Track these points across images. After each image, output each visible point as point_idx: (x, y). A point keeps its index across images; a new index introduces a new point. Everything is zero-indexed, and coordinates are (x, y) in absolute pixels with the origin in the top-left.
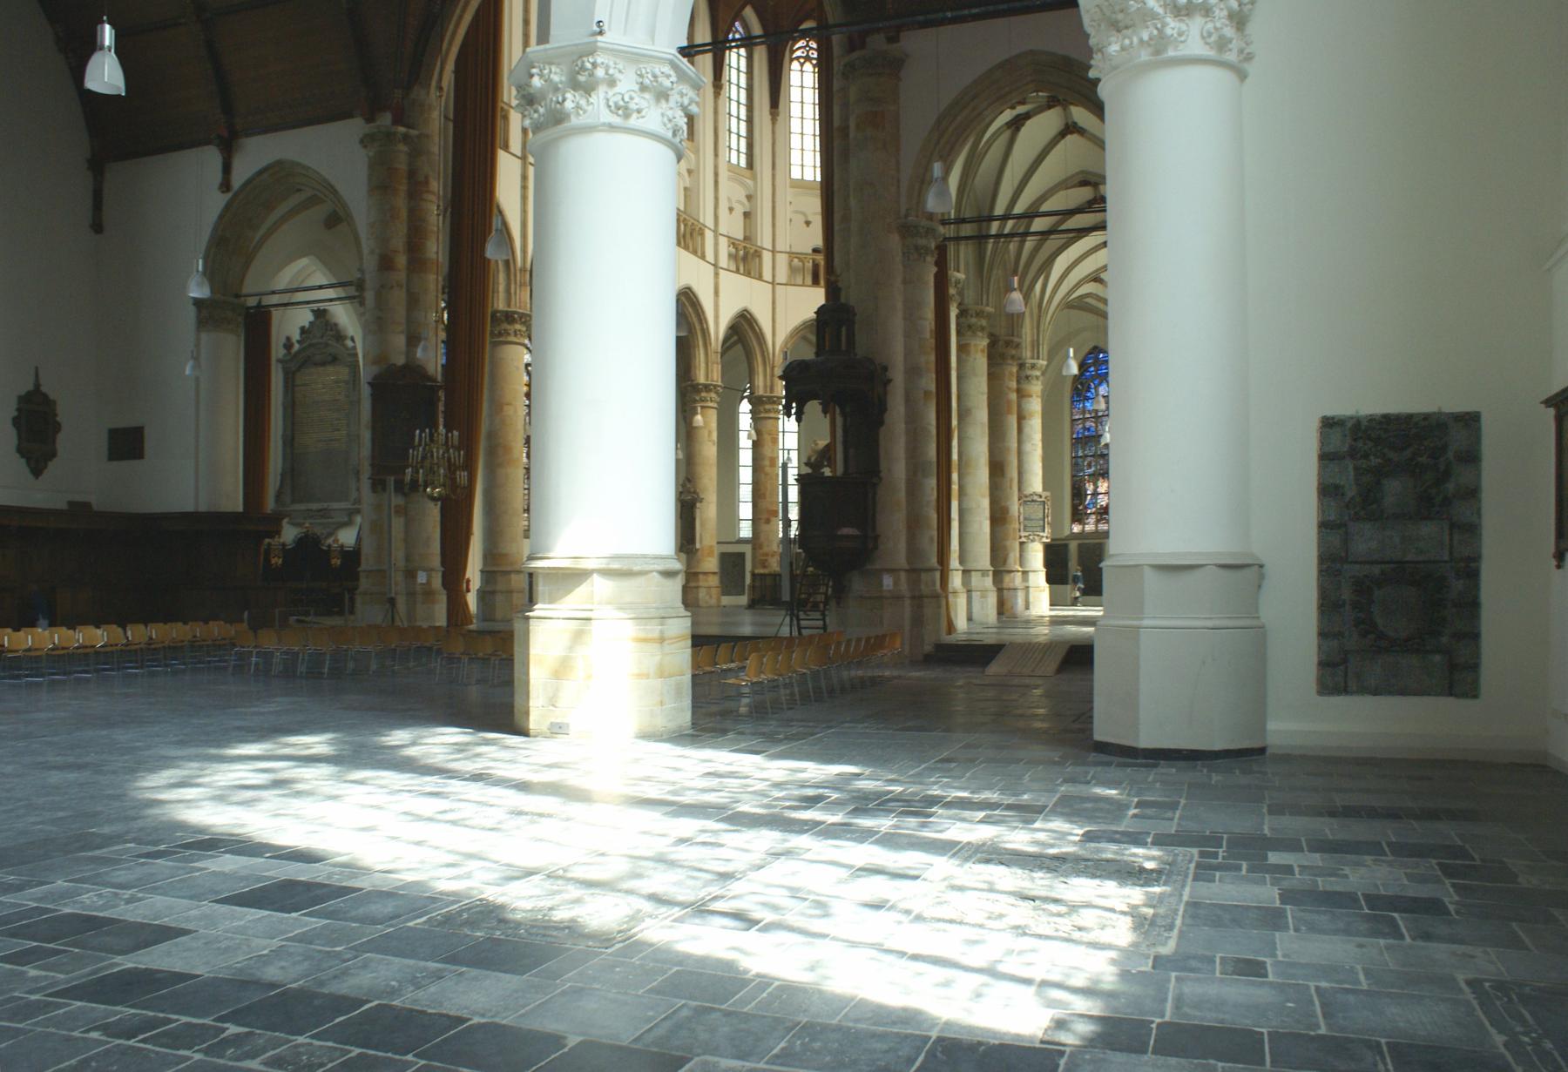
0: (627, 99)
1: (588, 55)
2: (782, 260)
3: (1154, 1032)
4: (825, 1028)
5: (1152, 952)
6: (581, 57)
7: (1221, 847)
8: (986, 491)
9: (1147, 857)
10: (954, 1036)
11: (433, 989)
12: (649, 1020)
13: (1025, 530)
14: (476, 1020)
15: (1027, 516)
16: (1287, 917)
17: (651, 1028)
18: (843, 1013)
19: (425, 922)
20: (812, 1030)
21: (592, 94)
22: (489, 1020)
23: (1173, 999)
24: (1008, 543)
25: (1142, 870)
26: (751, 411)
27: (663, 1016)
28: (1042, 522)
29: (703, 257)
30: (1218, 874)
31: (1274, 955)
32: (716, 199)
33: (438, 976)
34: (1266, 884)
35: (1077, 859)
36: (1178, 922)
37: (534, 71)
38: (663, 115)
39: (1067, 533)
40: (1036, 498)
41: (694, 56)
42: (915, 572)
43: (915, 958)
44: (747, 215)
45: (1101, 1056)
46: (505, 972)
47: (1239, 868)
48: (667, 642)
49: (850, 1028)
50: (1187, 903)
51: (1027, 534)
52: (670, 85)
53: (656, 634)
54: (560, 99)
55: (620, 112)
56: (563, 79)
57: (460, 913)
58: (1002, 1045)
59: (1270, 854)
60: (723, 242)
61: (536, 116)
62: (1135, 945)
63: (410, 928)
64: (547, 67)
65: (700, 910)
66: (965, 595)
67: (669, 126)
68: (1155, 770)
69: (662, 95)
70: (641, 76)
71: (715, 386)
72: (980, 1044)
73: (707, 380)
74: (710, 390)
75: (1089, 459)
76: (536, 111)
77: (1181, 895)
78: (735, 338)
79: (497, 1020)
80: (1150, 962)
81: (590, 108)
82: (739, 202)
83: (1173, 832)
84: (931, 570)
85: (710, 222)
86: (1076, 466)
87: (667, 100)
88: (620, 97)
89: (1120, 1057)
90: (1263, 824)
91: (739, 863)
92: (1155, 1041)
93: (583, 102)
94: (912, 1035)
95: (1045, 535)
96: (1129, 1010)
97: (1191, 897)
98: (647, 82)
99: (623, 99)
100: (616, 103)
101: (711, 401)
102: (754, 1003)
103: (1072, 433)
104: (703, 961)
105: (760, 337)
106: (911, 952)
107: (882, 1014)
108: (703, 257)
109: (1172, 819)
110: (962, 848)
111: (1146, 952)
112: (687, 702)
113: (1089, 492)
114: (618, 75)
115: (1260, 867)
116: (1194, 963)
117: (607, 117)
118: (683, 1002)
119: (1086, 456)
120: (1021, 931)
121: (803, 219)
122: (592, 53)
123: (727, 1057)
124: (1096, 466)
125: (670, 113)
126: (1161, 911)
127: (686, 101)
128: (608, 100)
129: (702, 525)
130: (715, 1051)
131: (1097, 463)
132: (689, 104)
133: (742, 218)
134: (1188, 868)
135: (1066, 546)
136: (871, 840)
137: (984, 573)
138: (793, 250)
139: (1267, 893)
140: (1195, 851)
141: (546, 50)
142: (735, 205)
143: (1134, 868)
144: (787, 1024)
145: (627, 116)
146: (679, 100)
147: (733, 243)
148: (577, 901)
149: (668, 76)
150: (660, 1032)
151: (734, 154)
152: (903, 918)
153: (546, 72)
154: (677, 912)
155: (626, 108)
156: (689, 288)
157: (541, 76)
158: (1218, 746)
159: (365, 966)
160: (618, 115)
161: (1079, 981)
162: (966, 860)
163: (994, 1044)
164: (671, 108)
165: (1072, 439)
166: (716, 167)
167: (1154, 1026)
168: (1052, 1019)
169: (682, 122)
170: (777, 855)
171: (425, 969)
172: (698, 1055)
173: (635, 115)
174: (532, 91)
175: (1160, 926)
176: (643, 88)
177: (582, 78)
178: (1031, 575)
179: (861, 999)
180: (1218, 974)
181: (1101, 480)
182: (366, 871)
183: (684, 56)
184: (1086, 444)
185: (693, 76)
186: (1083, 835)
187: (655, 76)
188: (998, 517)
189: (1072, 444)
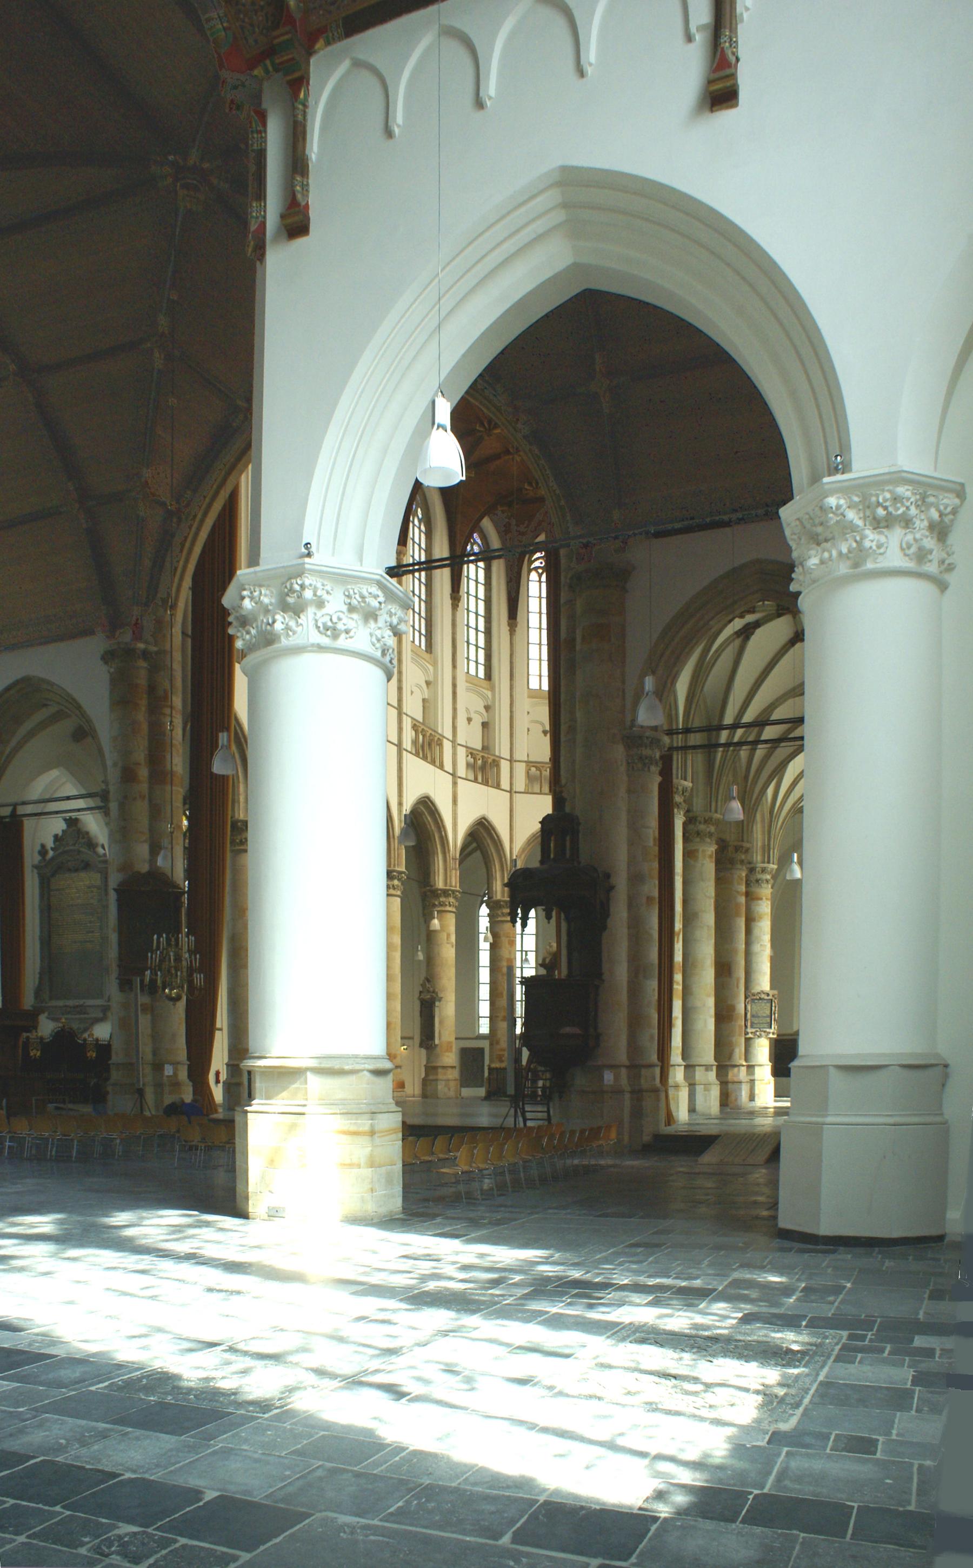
0: (335, 620)
1: (296, 578)
2: (520, 769)
3: (749, 1502)
4: (444, 1489)
5: (772, 1428)
6: (290, 579)
7: (872, 1330)
8: (712, 991)
9: (792, 1339)
10: (559, 1501)
11: (96, 1447)
12: (284, 1478)
13: (752, 1027)
14: (128, 1475)
15: (754, 1013)
16: (913, 1398)
17: (285, 1485)
18: (464, 1477)
19: (106, 1387)
20: (431, 1492)
21: (301, 616)
22: (139, 1476)
23: (778, 1472)
24: (734, 1039)
25: (789, 1351)
26: (489, 915)
27: (298, 1476)
28: (768, 1020)
29: (441, 767)
30: (859, 1355)
31: (890, 1434)
32: (455, 710)
33: (104, 1435)
34: (903, 1366)
35: (728, 1340)
36: (806, 1401)
37: (245, 593)
38: (371, 635)
40: (763, 996)
41: (402, 575)
42: (635, 1067)
43: (545, 1430)
44: (485, 725)
45: (692, 1523)
46: (166, 1433)
47: (882, 1350)
48: (377, 1135)
49: (466, 1491)
50: (821, 1383)
51: (754, 1030)
52: (377, 605)
53: (366, 1128)
54: (270, 621)
55: (329, 633)
56: (273, 601)
57: (140, 1379)
58: (602, 1510)
59: (917, 1338)
60: (461, 752)
61: (248, 637)
62: (758, 1421)
63: (91, 1391)
64: (257, 589)
65: (355, 1382)
66: (687, 1089)
67: (378, 645)
68: (832, 1256)
69: (370, 615)
70: (349, 596)
71: (453, 891)
72: (582, 1508)
74: (449, 895)
76: (248, 633)
77: (818, 1375)
78: (474, 845)
79: (147, 1476)
80: (767, 1437)
81: (300, 628)
82: (476, 712)
83: (830, 1315)
84: (652, 1066)
85: (448, 733)
87: (376, 620)
88: (329, 618)
89: (709, 1525)
90: (920, 1309)
91: (405, 1339)
92: (748, 1511)
93: (292, 624)
94: (522, 1498)
95: (772, 1031)
96: (732, 1482)
97: (826, 1377)
98: (354, 602)
99: (331, 620)
100: (324, 624)
101: (450, 906)
102: (384, 1466)
104: (349, 1429)
105: (498, 843)
106: (542, 1424)
107: (497, 1480)
108: (441, 767)
109: (832, 1303)
110: (623, 1328)
111: (767, 1428)
112: (398, 1189)
114: (325, 597)
115: (904, 1350)
116: (808, 1440)
117: (317, 638)
118: (321, 1463)
120: (653, 1407)
121: (541, 729)
122: (300, 575)
123: (346, 1514)
125: (378, 633)
126: (793, 1391)
127: (395, 621)
128: (316, 621)
129: (441, 1022)
130: (339, 1509)
132: (398, 624)
133: (480, 728)
134: (832, 1350)
136: (539, 1319)
137: (708, 1068)
138: (531, 759)
139: (903, 1375)
140: (845, 1334)
141: (255, 572)
142: (473, 716)
143: (782, 1347)
144: (411, 1485)
145: (335, 637)
146: (388, 619)
147: (471, 752)
148: (245, 1372)
149: (376, 597)
150: (290, 1489)
151: (472, 665)
152: (545, 1392)
153: (256, 594)
154: (336, 1383)
155: (335, 629)
156: (428, 798)
157: (252, 598)
158: (896, 1234)
159: (40, 1425)
160: (326, 636)
161: (692, 1455)
162: (623, 1339)
163: (595, 1509)
164: (379, 628)
166: (454, 678)
167: (751, 1497)
168: (654, 1490)
169: (391, 641)
170: (445, 1333)
171: (94, 1429)
172: (320, 1511)
173: (343, 636)
174: (244, 613)
175: (788, 1404)
176: (351, 609)
177: (291, 600)
178: (757, 1069)
179: (481, 1468)
180: (828, 1451)
182: (54, 1342)
183: (392, 576)
185: (401, 594)
186: (741, 1319)
187: (363, 597)
188: (724, 1015)
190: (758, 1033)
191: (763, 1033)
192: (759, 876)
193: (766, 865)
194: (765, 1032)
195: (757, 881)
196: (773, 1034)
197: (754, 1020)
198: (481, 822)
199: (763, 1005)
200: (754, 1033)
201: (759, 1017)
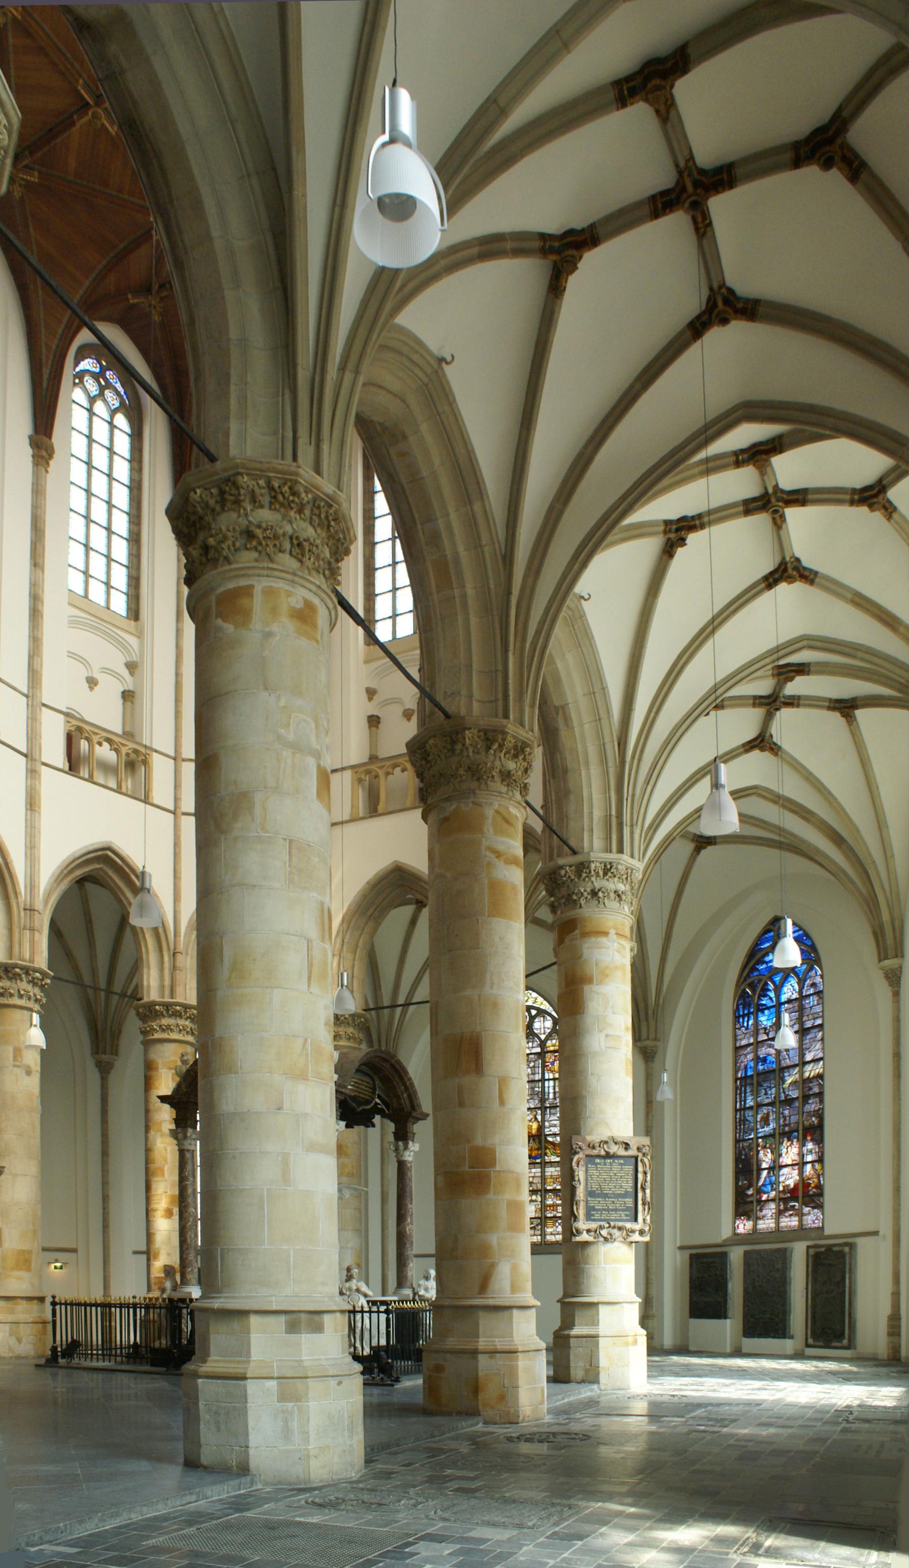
13: (589, 1217)
15: (595, 1187)
24: (493, 1239)
39: (726, 1233)
40: (613, 1149)
51: (593, 1225)
73: (11, 956)
74: (17, 977)
75: (765, 1110)
86: (741, 1123)
103: (736, 1071)
113: (764, 1165)
119: (759, 1106)
124: (777, 1120)
131: (779, 1114)
135: (724, 1255)
165: (737, 1079)
181: (786, 1143)
184: (759, 1084)
189: (737, 1088)
190: (604, 1232)
191: (616, 1232)
192: (598, 883)
193: (613, 856)
194: (620, 1229)
195: (594, 893)
196: (642, 1232)
197: (593, 1202)
198: (107, 856)
199: (616, 1168)
200: (596, 1232)
201: (606, 1196)
